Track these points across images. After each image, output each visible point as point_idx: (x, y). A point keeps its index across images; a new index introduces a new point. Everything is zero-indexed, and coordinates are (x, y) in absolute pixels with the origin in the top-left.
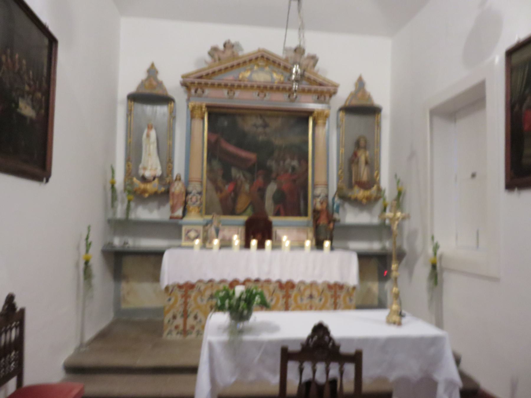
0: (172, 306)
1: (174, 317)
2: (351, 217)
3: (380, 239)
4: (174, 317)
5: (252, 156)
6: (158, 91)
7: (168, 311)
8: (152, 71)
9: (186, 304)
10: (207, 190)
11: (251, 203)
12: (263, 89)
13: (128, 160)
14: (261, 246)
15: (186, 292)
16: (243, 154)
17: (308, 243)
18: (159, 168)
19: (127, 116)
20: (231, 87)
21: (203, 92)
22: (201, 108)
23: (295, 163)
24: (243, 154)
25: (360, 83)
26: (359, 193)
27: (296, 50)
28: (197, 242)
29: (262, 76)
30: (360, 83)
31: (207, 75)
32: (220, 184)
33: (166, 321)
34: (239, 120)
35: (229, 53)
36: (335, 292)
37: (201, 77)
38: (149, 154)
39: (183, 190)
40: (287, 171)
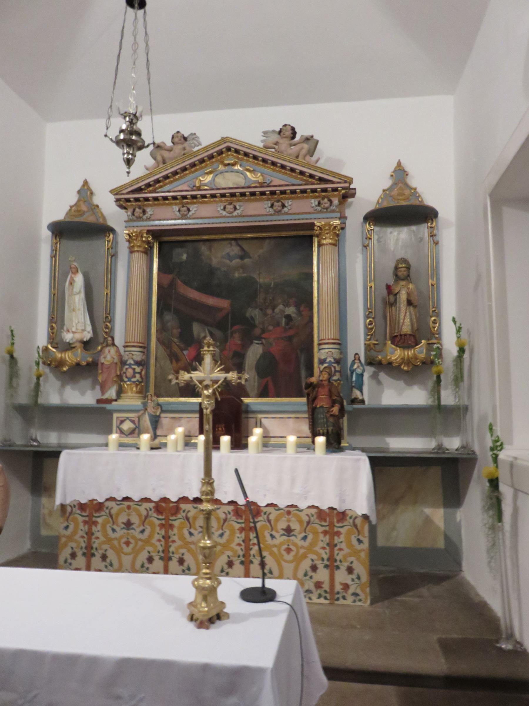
0: (70, 538)
2: (396, 394)
3: (431, 433)
5: (224, 304)
6: (89, 218)
7: (65, 545)
8: (86, 191)
10: (156, 359)
12: (233, 196)
13: (52, 320)
15: (90, 516)
16: (211, 301)
17: (292, 439)
18: (89, 328)
19: (52, 258)
20: (184, 201)
21: (144, 212)
22: (142, 237)
23: (291, 310)
24: (211, 301)
25: (400, 173)
26: (396, 354)
27: (280, 132)
28: (146, 437)
29: (230, 179)
30: (400, 173)
31: (148, 185)
32: (176, 349)
34: (204, 249)
35: (178, 149)
36: (331, 525)
37: (139, 190)
38: (74, 310)
39: (116, 360)
40: (278, 324)
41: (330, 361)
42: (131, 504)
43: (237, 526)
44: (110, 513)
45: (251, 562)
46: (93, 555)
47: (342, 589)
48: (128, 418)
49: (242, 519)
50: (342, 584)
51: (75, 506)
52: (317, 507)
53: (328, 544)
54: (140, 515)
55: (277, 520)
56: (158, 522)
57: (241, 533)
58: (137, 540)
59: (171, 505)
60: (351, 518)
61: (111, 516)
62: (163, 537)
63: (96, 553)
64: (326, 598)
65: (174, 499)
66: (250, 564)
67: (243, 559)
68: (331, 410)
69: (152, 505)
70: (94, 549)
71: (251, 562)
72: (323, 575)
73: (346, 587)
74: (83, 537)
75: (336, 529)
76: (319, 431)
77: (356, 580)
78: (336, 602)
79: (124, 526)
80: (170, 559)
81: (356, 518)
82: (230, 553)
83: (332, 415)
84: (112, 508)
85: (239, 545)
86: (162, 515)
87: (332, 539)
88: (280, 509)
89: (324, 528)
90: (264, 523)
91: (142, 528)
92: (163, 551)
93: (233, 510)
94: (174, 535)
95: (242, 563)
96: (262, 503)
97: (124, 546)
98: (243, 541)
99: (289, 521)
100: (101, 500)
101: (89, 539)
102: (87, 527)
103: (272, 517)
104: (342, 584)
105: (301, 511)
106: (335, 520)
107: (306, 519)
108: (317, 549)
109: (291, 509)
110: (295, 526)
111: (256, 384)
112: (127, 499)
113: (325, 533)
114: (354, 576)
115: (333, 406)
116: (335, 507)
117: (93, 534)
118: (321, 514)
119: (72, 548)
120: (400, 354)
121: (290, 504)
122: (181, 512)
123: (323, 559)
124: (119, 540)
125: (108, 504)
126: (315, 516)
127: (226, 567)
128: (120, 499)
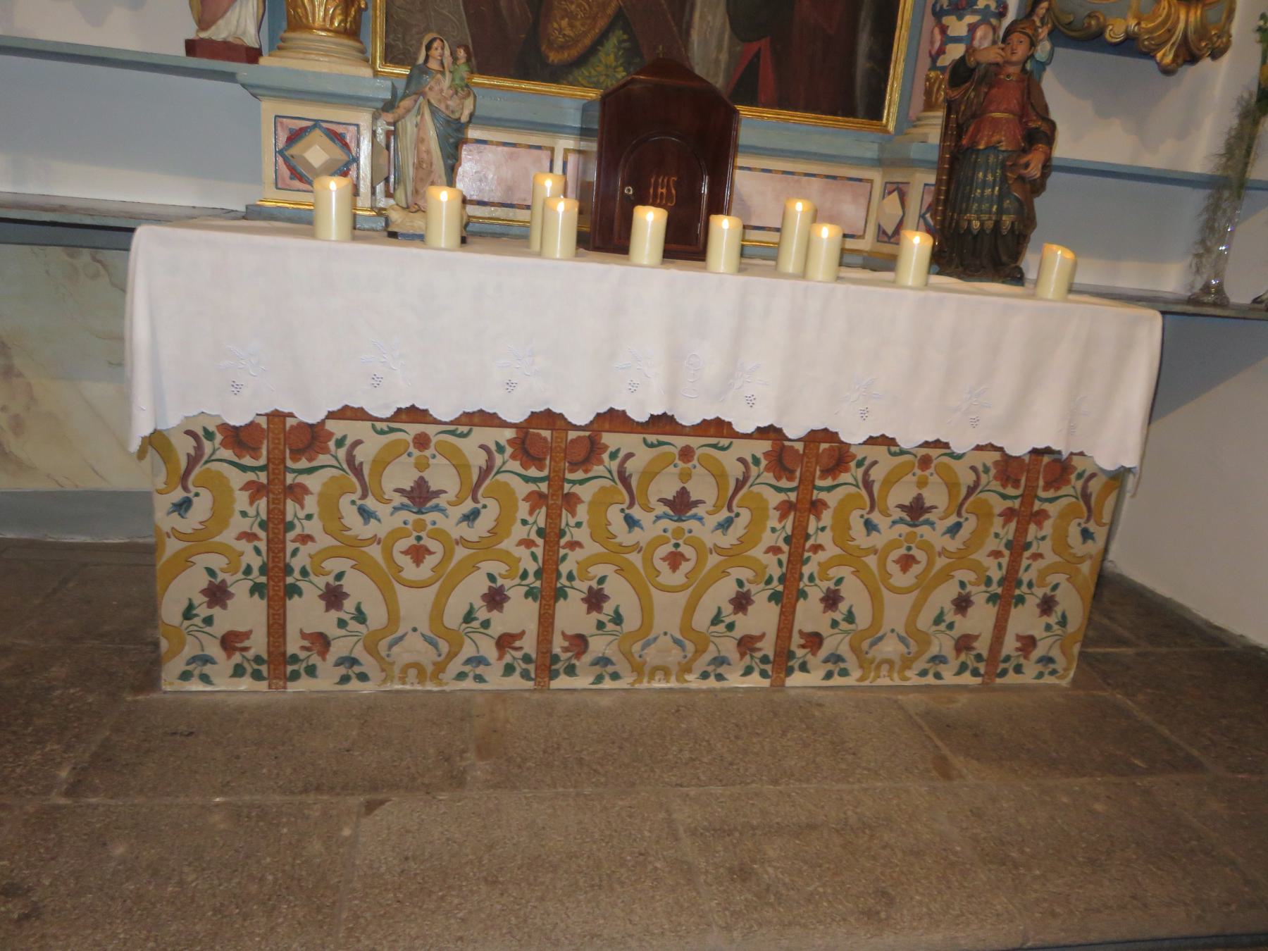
0: (200, 540)
1: (217, 594)
4: (217, 594)
7: (183, 562)
9: (276, 525)
11: (620, 19)
14: (685, 243)
15: (275, 467)
33: (171, 611)
36: (1029, 496)
41: (987, 6)
42: (430, 430)
43: (775, 499)
44: (350, 459)
45: (803, 594)
46: (294, 590)
47: (1018, 649)
48: (317, 123)
49: (790, 479)
50: (1019, 638)
51: (209, 435)
52: (1001, 449)
53: (1009, 545)
54: (461, 467)
55: (889, 482)
56: (522, 489)
57: (783, 517)
58: (450, 545)
59: (572, 435)
60: (1080, 476)
61: (357, 471)
62: (540, 532)
63: (303, 585)
64: (975, 673)
65: (579, 414)
66: (797, 600)
67: (780, 588)
68: (1024, 160)
69: (510, 434)
70: (297, 574)
71: (803, 594)
72: (980, 619)
73: (1028, 643)
74: (249, 536)
75: (1037, 506)
76: (969, 222)
77: (1056, 627)
78: (998, 681)
79: (406, 501)
80: (561, 594)
81: (1093, 475)
82: (745, 574)
83: (1021, 178)
84: (358, 443)
85: (775, 550)
86: (541, 469)
87: (1021, 531)
88: (903, 452)
89: (1009, 503)
90: (853, 490)
91: (469, 505)
92: (538, 574)
93: (766, 454)
94: (579, 525)
95: (775, 597)
96: (854, 435)
97: (405, 562)
98: (788, 540)
99: (922, 483)
100: (311, 415)
101: (276, 546)
102: (262, 503)
103: (877, 475)
104: (1019, 638)
105: (960, 457)
106: (1041, 483)
107: (969, 478)
108: (981, 556)
109: (934, 453)
110: (936, 496)
111: (724, 57)
112: (414, 414)
113: (1008, 514)
114: (1053, 620)
115: (1024, 151)
116: (1055, 448)
117: (290, 526)
118: (1009, 468)
119: (211, 572)
120: (1168, 15)
121: (930, 439)
122: (605, 456)
123: (989, 581)
124: (387, 544)
125: (334, 427)
126: (993, 472)
127: (728, 609)
128: (388, 413)
